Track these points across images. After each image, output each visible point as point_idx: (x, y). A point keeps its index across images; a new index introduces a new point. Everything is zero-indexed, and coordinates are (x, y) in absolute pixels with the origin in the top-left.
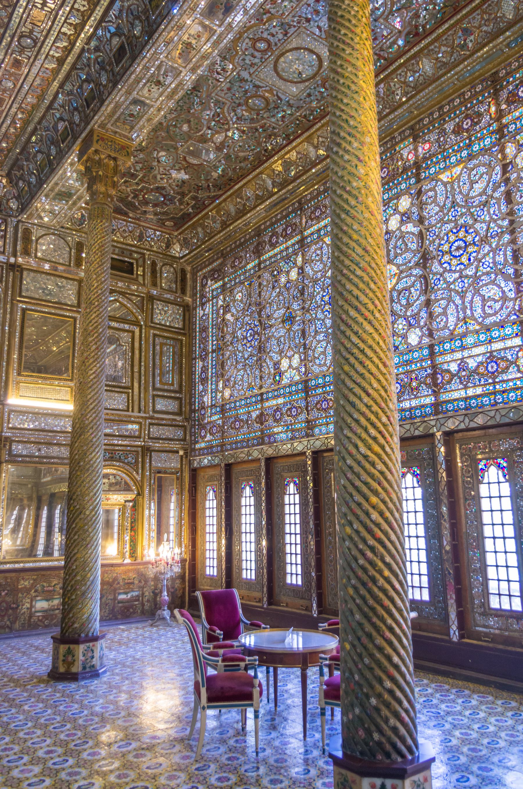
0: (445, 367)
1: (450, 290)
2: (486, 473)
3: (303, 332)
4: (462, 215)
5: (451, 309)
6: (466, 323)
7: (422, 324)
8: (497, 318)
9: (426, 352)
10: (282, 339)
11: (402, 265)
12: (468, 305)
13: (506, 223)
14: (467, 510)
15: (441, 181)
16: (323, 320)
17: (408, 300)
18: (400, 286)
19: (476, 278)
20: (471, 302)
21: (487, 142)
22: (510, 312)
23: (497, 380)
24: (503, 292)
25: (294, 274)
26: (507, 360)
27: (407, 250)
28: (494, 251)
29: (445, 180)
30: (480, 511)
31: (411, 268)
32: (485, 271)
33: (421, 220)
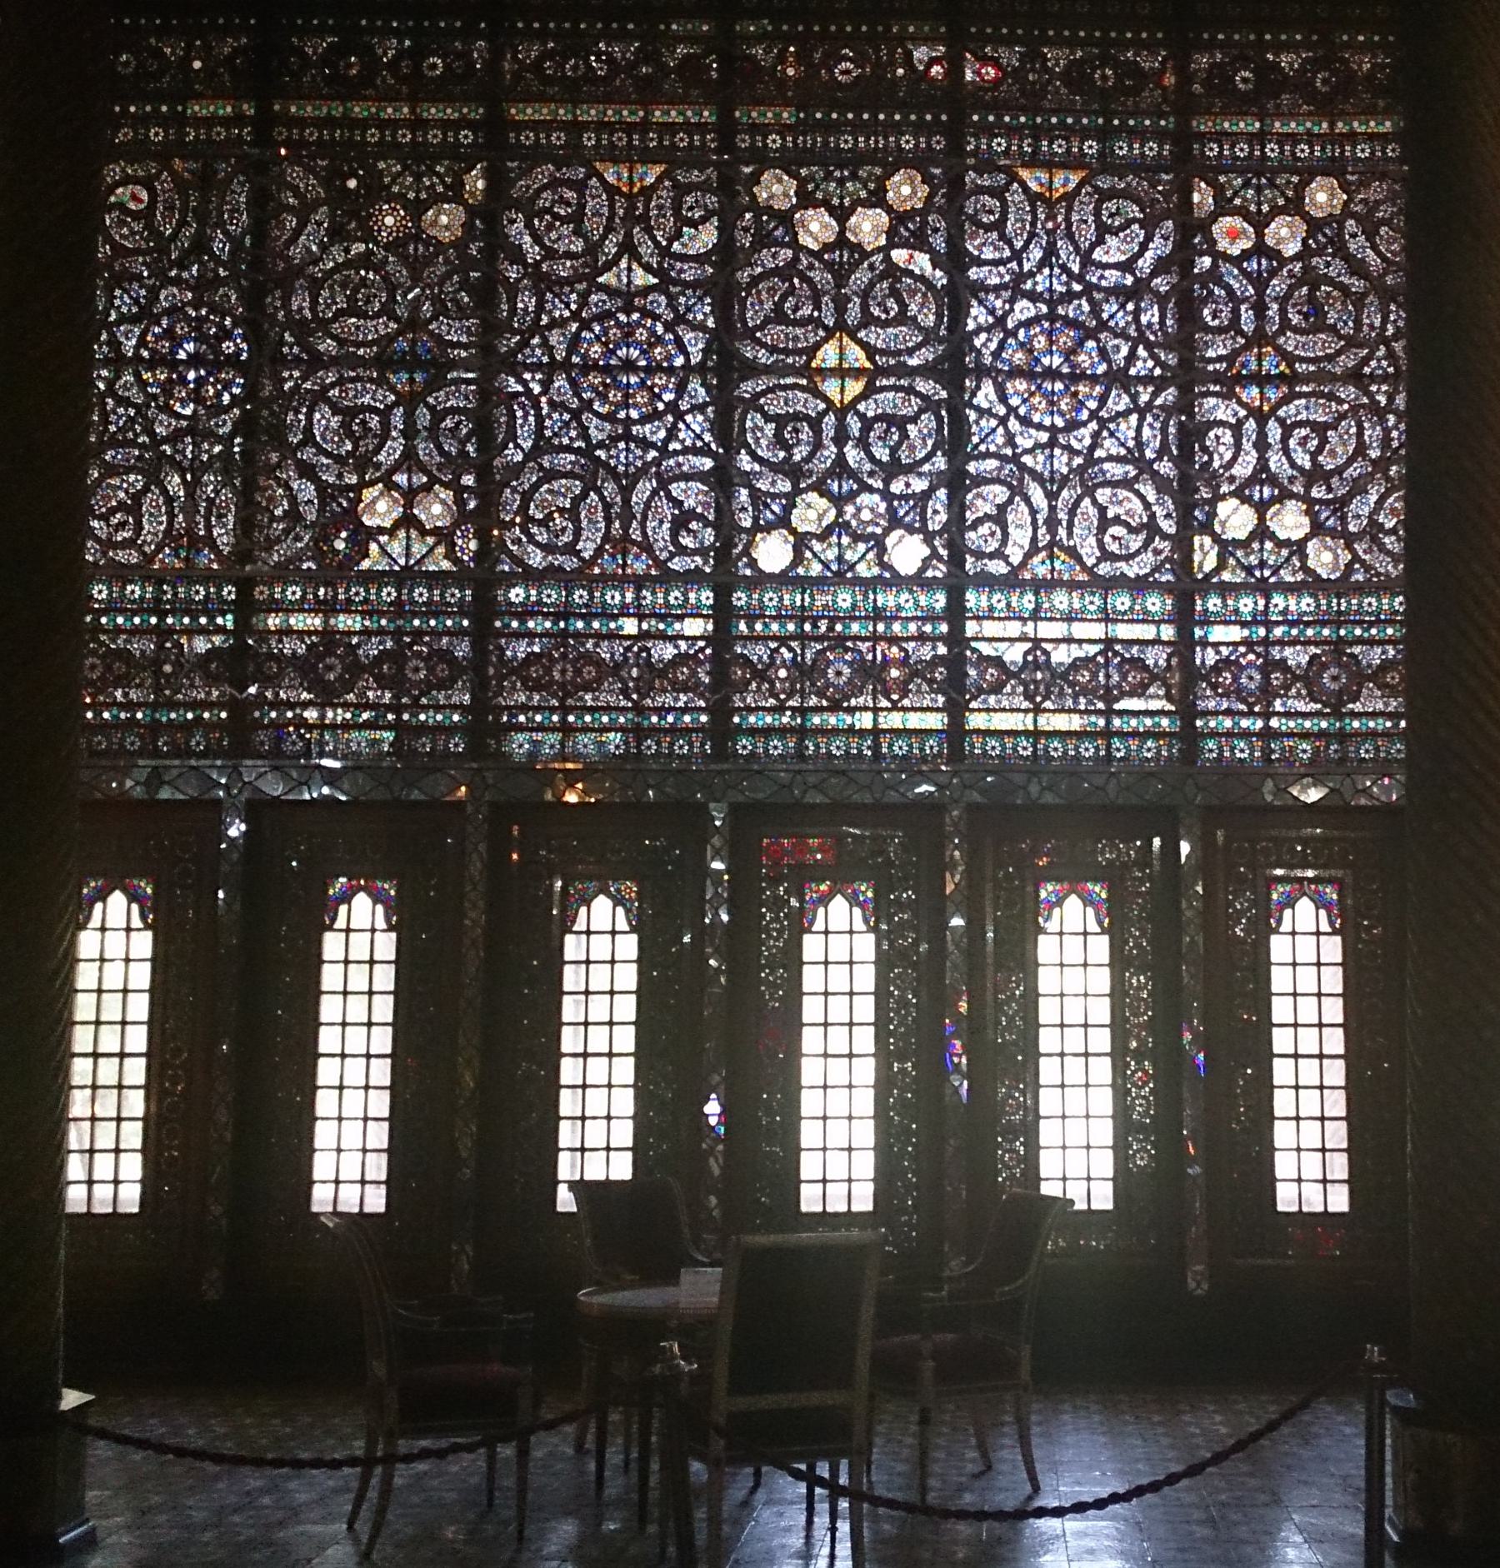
0: (986, 649)
1: (1023, 468)
2: (1056, 911)
3: (484, 430)
4: (1070, 296)
5: (1019, 515)
6: (1051, 557)
7: (934, 525)
8: (1132, 570)
9: (940, 600)
10: (374, 422)
11: (883, 352)
12: (1063, 516)
13: (1172, 359)
14: (996, 992)
15: (1023, 184)
16: (576, 415)
17: (894, 451)
18: (869, 408)
19: (1091, 461)
20: (1072, 512)
21: (1151, 149)
22: (1163, 563)
23: (1116, 706)
24: (1153, 516)
25: (445, 221)
26: (1146, 668)
27: (903, 318)
28: (1142, 412)
29: (1034, 186)
30: (1031, 998)
31: (914, 372)
32: (1114, 451)
33: (956, 260)
